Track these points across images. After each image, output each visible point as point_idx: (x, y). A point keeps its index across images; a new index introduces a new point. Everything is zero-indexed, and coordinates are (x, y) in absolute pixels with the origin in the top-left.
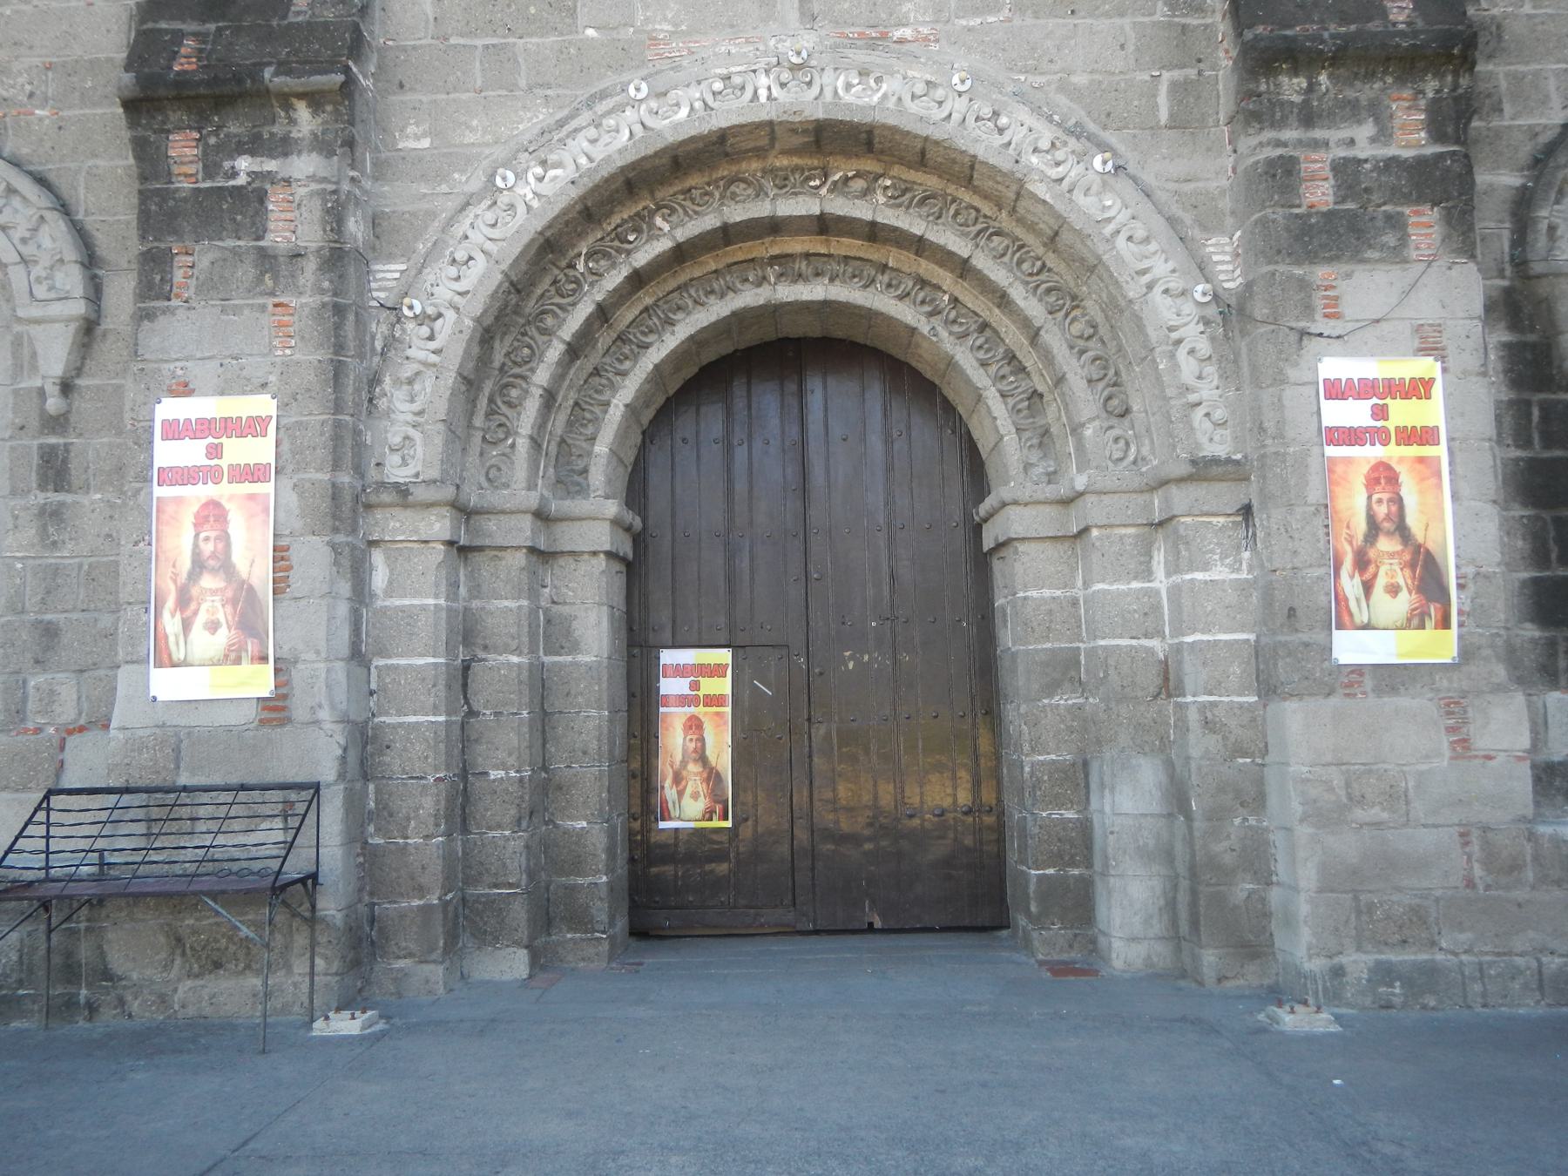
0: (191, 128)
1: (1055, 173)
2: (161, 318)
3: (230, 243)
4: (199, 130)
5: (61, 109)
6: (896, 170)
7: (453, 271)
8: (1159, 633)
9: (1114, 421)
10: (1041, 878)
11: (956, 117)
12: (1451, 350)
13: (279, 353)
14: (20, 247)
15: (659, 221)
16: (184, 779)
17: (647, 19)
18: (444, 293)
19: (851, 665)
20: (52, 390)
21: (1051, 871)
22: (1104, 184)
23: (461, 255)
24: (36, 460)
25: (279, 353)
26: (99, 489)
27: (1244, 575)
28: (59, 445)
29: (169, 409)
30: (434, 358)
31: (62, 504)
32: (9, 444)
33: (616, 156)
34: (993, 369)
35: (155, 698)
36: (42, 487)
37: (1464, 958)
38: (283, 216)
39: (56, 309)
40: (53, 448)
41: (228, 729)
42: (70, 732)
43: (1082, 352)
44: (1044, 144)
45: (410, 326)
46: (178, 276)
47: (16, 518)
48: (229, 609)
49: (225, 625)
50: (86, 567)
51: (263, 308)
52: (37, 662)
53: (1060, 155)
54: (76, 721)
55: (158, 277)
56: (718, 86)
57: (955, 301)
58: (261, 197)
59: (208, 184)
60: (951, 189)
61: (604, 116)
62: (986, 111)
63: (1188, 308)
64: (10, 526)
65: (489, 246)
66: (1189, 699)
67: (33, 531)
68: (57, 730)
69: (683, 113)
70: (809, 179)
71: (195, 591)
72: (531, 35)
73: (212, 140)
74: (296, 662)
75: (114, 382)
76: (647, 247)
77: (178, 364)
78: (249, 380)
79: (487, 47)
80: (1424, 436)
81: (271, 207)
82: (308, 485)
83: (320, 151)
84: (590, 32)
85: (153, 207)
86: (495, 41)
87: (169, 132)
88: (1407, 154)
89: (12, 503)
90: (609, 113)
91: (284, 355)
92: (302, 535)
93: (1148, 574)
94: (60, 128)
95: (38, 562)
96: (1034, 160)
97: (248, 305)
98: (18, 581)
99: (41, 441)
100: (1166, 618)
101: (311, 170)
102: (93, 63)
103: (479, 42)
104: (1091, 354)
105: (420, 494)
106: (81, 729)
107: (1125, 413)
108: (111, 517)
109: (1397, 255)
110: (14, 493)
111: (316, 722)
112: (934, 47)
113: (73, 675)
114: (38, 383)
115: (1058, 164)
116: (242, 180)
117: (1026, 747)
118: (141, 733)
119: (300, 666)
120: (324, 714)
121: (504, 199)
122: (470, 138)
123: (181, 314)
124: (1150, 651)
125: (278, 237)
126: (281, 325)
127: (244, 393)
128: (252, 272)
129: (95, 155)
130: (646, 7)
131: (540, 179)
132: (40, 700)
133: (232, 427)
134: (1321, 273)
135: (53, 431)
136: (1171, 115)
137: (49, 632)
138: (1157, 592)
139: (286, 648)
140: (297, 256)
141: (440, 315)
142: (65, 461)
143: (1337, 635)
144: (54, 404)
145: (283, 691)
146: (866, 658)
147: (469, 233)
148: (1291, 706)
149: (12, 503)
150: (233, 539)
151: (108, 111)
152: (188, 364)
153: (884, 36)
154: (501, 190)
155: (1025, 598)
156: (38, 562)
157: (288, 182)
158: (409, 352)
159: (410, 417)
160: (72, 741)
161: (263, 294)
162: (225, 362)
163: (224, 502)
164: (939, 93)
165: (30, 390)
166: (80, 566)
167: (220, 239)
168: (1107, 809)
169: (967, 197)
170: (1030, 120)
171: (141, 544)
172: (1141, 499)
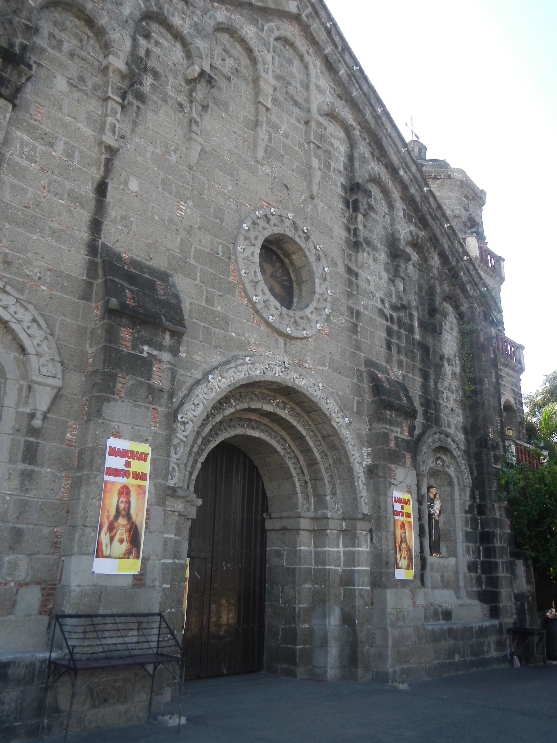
0: (130, 328)
1: (338, 420)
2: (112, 402)
3: (139, 378)
4: (132, 329)
5: (52, 290)
6: (291, 403)
7: (193, 407)
8: (339, 565)
9: (333, 496)
10: (300, 649)
11: (319, 396)
12: (412, 493)
13: (153, 428)
14: (37, 348)
15: (232, 401)
16: (101, 611)
17: (248, 336)
18: (190, 415)
19: (225, 568)
20: (39, 415)
21: (301, 646)
22: (347, 426)
23: (196, 402)
24: (22, 447)
25: (153, 428)
26: (49, 467)
27: (368, 550)
28: (34, 442)
29: (113, 442)
30: (184, 439)
31: (33, 471)
32: (11, 437)
33: (241, 380)
34: (297, 470)
35: (93, 572)
36: (24, 461)
37: (415, 665)
38: (158, 374)
39: (51, 381)
40: (31, 442)
41: (121, 588)
42: (21, 585)
43: (328, 473)
44: (336, 411)
45: (179, 424)
46: (119, 386)
47: (10, 474)
48: (128, 533)
49: (125, 541)
50: (40, 503)
51: (148, 408)
52: (11, 548)
53: (339, 415)
54: (25, 579)
55: (112, 385)
56: (267, 366)
57: (289, 446)
58: (151, 364)
59: (133, 352)
60: (302, 413)
61: (240, 365)
62: (325, 397)
63: (361, 468)
64: (7, 477)
65: (205, 401)
66: (356, 587)
67: (18, 482)
68: (15, 584)
69: (258, 372)
70: (271, 399)
71: (116, 524)
72: (217, 327)
73: (136, 335)
74: (148, 559)
75: (63, 418)
76: (229, 409)
77: (116, 423)
78: (141, 436)
79: (204, 327)
80: (408, 515)
81: (154, 369)
82: (158, 485)
83: (172, 353)
84: (233, 334)
85: (113, 355)
86: (206, 325)
87: (121, 326)
88: (406, 438)
89: (10, 466)
90: (240, 365)
91: (154, 430)
92: (154, 505)
93: (338, 546)
94: (51, 298)
95: (18, 497)
96: (334, 415)
97: (144, 406)
98: (6, 506)
99: (26, 438)
100: (342, 561)
101: (168, 359)
102: (68, 277)
103: (202, 324)
104: (329, 474)
105: (180, 492)
106: (27, 584)
107: (336, 493)
108: (54, 481)
109: (404, 465)
110: (11, 461)
111: (153, 587)
112: (313, 372)
113: (25, 556)
114: (28, 410)
115: (338, 418)
116: (145, 355)
117: (297, 602)
118: (86, 588)
119: (150, 562)
120: (157, 583)
121: (210, 385)
122: (198, 358)
123: (119, 402)
124: (338, 571)
125: (155, 381)
126: (155, 417)
127: (139, 442)
128: (146, 393)
129: (65, 316)
130: (248, 332)
131: (220, 381)
132: (10, 568)
133: (134, 455)
134: (393, 466)
135: (33, 436)
136: (357, 410)
137: (18, 534)
138: (339, 552)
139: (146, 553)
140: (162, 391)
141: (187, 423)
142: (36, 451)
143: (397, 571)
144: (37, 423)
145: (143, 572)
146: (229, 565)
147: (199, 394)
148: (388, 591)
149: (10, 466)
150: (131, 503)
151: (72, 298)
152: (120, 424)
153: (302, 365)
154: (209, 382)
155: (300, 550)
156: (18, 497)
157: (160, 361)
158: (178, 435)
159: (175, 461)
160: (23, 590)
161: (149, 403)
162: (134, 427)
163: (130, 487)
164: (316, 388)
165: (23, 413)
166: (37, 502)
167: (136, 376)
168: (327, 623)
169: (306, 418)
170: (334, 403)
171: (94, 500)
172: (340, 522)
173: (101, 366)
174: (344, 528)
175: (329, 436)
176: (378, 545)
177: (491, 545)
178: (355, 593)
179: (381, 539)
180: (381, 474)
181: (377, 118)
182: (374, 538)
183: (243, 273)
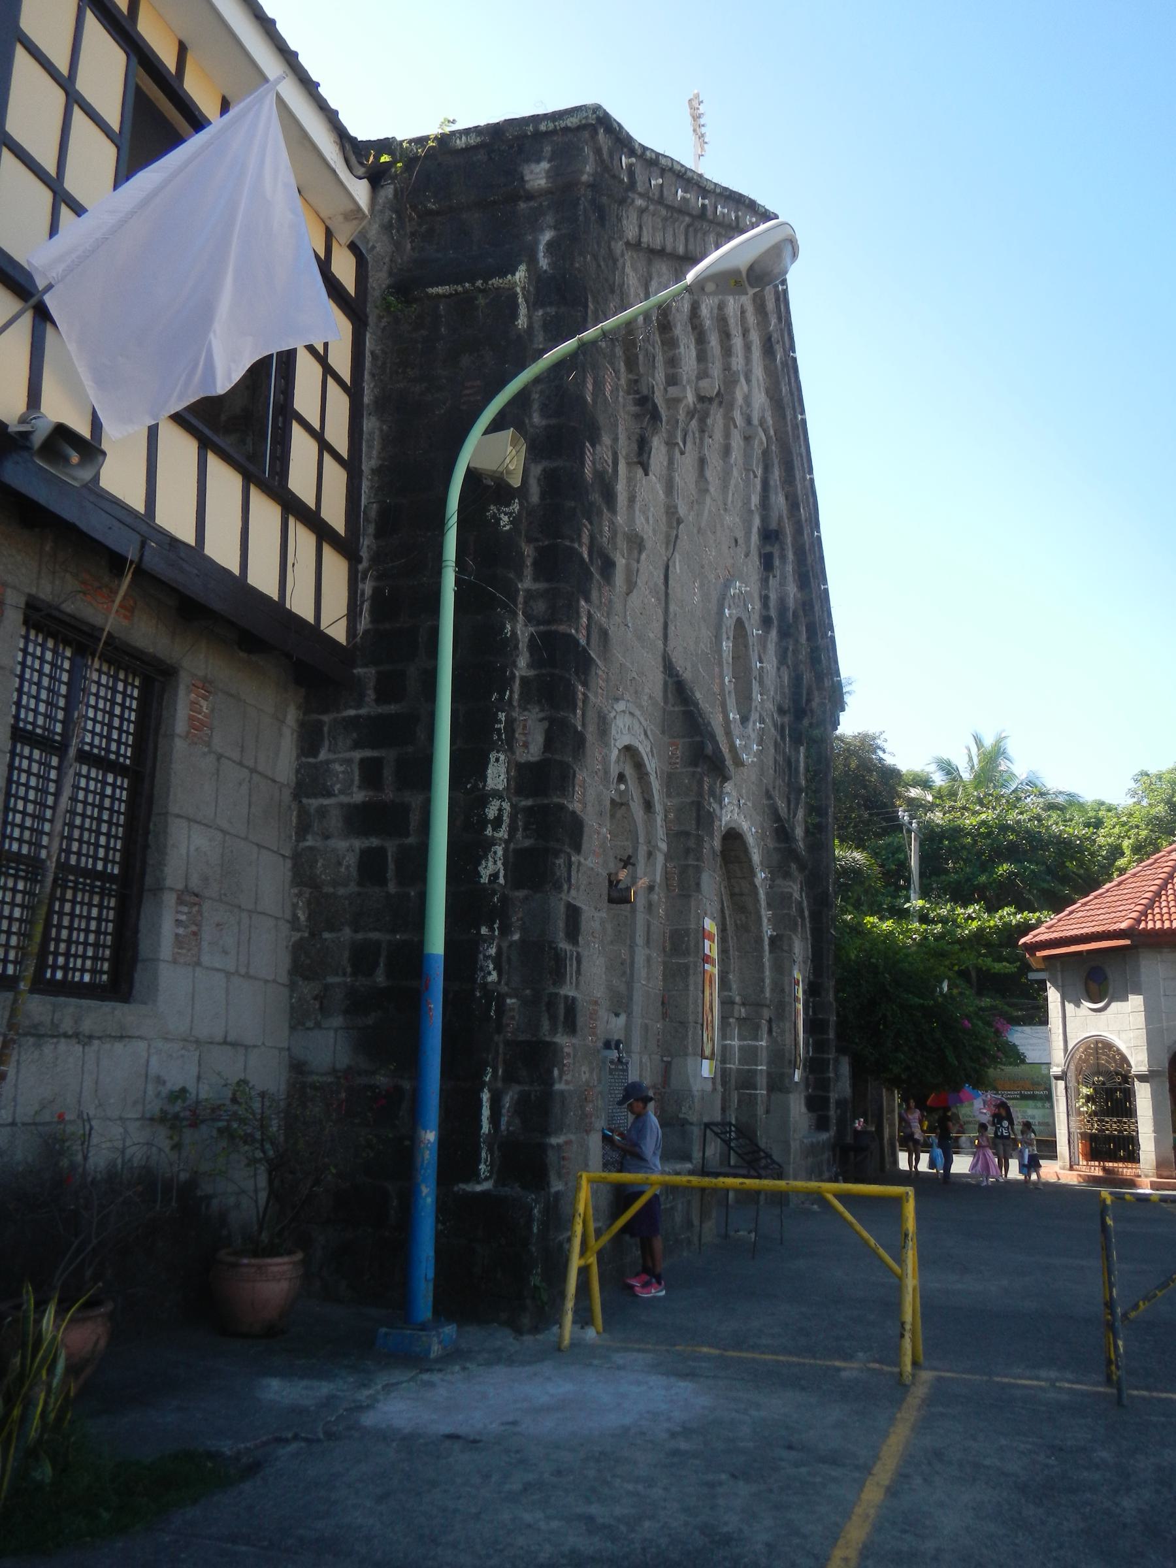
148: (792, 1096)
173: (694, 827)
174: (743, 1015)
175: (742, 895)
176: (779, 1039)
177: (825, 1037)
178: (756, 1099)
179: (783, 1032)
180: (786, 948)
181: (795, 427)
182: (775, 1029)
183: (727, 679)
